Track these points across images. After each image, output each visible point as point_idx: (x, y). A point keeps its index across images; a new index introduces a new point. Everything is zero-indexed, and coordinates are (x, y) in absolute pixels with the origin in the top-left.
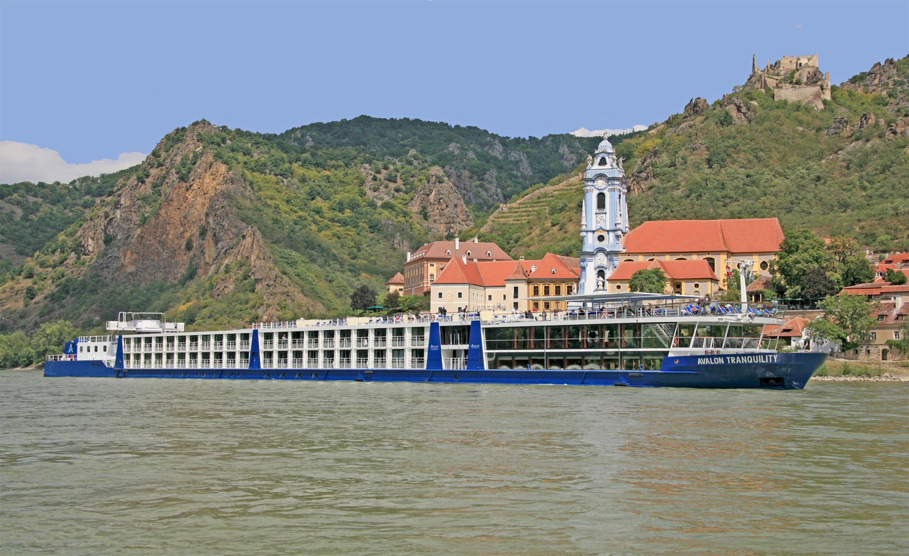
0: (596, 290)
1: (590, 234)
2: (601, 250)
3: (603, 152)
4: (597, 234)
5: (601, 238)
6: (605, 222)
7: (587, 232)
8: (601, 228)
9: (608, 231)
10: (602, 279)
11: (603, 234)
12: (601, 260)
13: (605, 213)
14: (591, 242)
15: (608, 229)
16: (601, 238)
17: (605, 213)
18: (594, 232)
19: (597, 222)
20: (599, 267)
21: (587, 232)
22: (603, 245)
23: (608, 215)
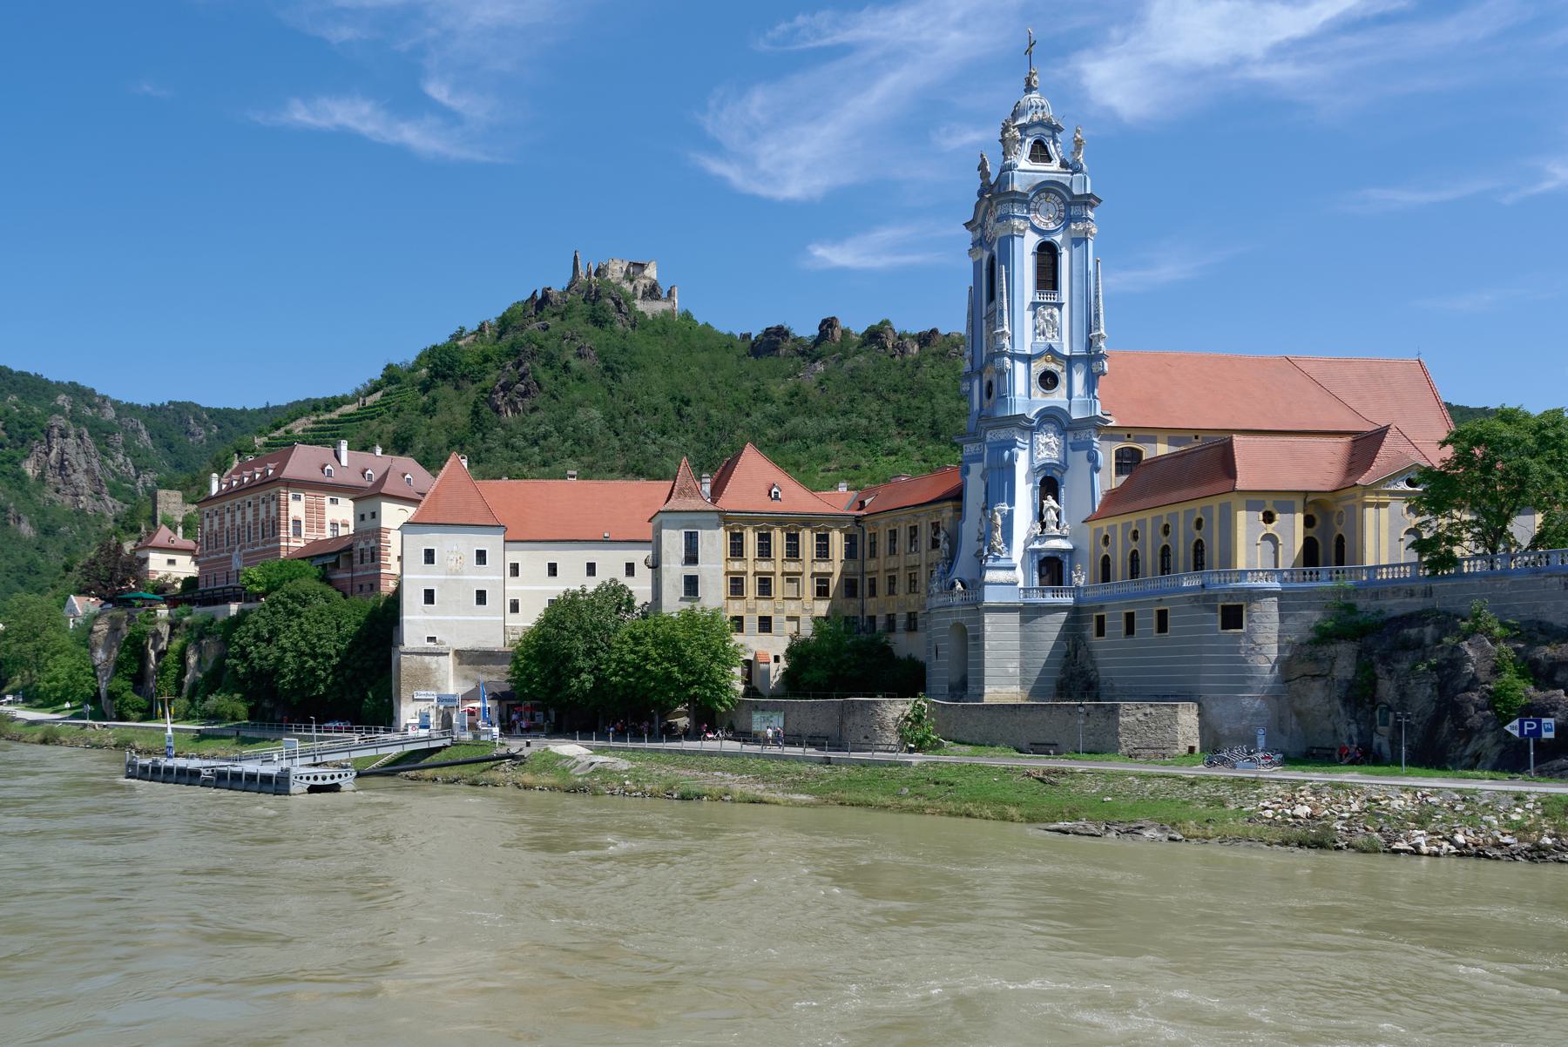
0: (1042, 537)
1: (1020, 367)
2: (1052, 418)
3: (1041, 123)
4: (1038, 367)
5: (1048, 380)
6: (1059, 333)
7: (1013, 357)
8: (1050, 350)
9: (1070, 361)
10: (1053, 503)
11: (1052, 367)
12: (1048, 447)
13: (1059, 306)
14: (1024, 395)
15: (1066, 352)
16: (1048, 380)
17: (1059, 306)
18: (1028, 359)
19: (1039, 332)
20: (1044, 467)
21: (1013, 357)
22: (1058, 397)
23: (1065, 308)
